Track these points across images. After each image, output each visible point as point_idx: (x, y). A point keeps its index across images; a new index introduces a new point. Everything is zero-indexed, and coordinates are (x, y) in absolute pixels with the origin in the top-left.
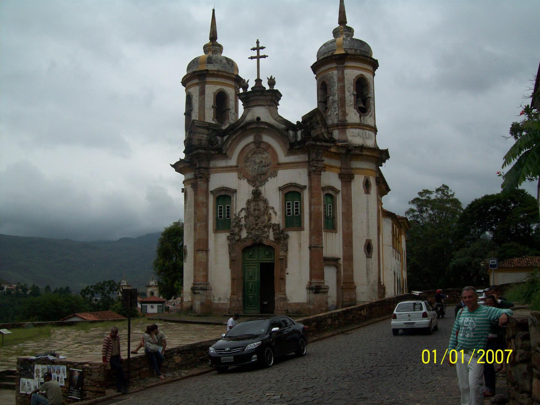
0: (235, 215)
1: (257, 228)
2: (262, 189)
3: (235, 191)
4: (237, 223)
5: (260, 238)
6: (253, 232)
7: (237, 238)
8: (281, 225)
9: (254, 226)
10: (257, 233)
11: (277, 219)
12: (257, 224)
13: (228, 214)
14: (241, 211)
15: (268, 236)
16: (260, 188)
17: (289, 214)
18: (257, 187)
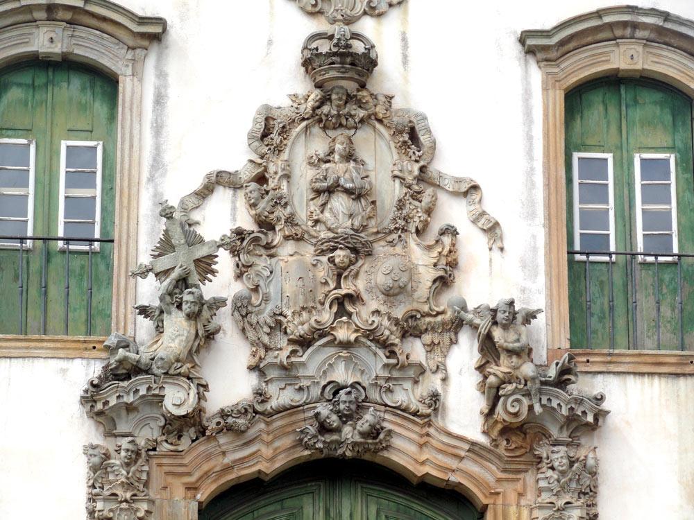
0: (167, 214)
1: (343, 334)
2: (380, 35)
3: (153, 34)
4: (183, 282)
5: (368, 418)
6: (313, 362)
7: (177, 399)
8: (541, 320)
9: (326, 316)
10: (341, 374)
11: (510, 267)
12: (343, 304)
13: (77, 206)
14: (205, 192)
15: (435, 399)
16: (367, 26)
17: (596, 244)
18: (349, 21)
